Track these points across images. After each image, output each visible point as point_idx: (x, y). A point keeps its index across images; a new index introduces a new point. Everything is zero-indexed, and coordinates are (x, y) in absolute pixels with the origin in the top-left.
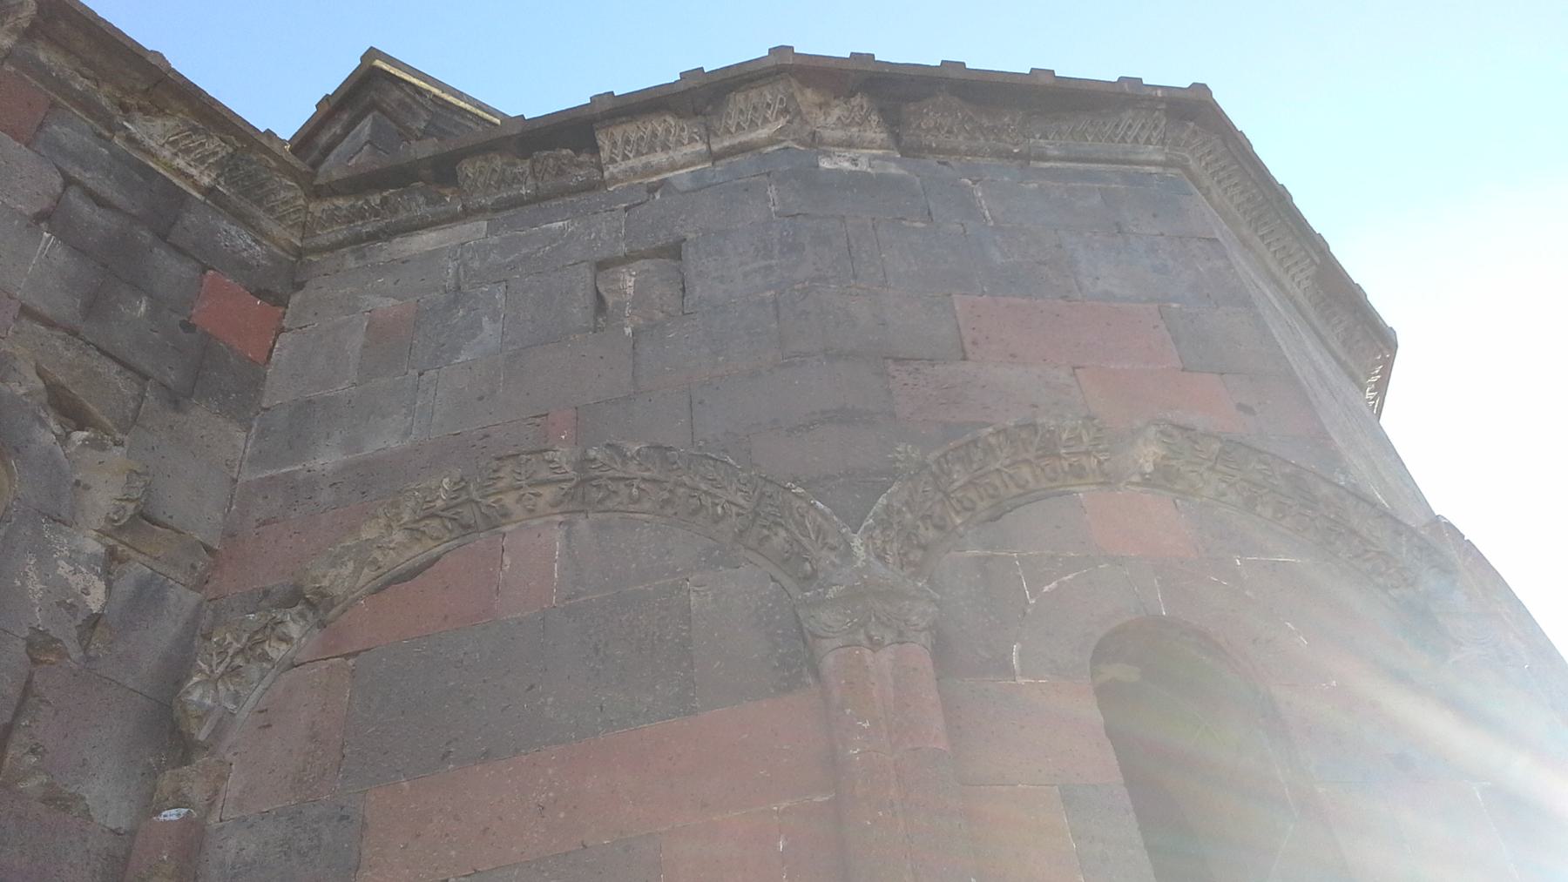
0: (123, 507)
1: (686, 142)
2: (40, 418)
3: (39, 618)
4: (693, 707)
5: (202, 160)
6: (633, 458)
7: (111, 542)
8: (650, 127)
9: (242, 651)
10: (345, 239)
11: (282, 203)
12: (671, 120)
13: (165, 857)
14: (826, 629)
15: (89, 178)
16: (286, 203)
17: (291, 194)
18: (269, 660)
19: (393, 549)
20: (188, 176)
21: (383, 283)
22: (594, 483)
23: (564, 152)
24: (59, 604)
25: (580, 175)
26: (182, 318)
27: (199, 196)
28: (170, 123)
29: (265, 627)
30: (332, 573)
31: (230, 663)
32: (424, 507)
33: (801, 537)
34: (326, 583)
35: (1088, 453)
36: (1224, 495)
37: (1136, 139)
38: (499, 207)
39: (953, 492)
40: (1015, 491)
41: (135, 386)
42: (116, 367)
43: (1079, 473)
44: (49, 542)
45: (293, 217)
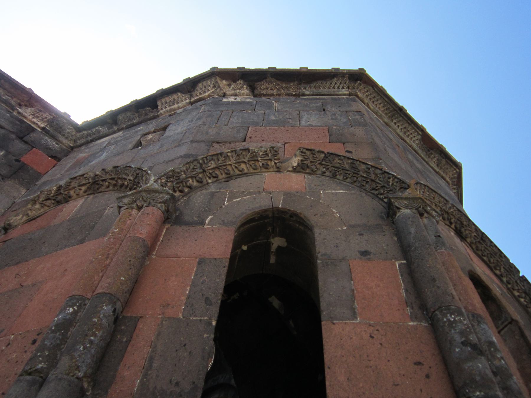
1: (184, 100)
5: (42, 120)
10: (84, 142)
12: (179, 94)
16: (68, 133)
17: (70, 131)
19: (34, 210)
20: (37, 124)
22: (96, 183)
23: (148, 108)
25: (152, 114)
27: (40, 130)
28: (33, 109)
30: (15, 218)
35: (271, 160)
36: (324, 173)
37: (338, 88)
40: (237, 172)
43: (266, 167)
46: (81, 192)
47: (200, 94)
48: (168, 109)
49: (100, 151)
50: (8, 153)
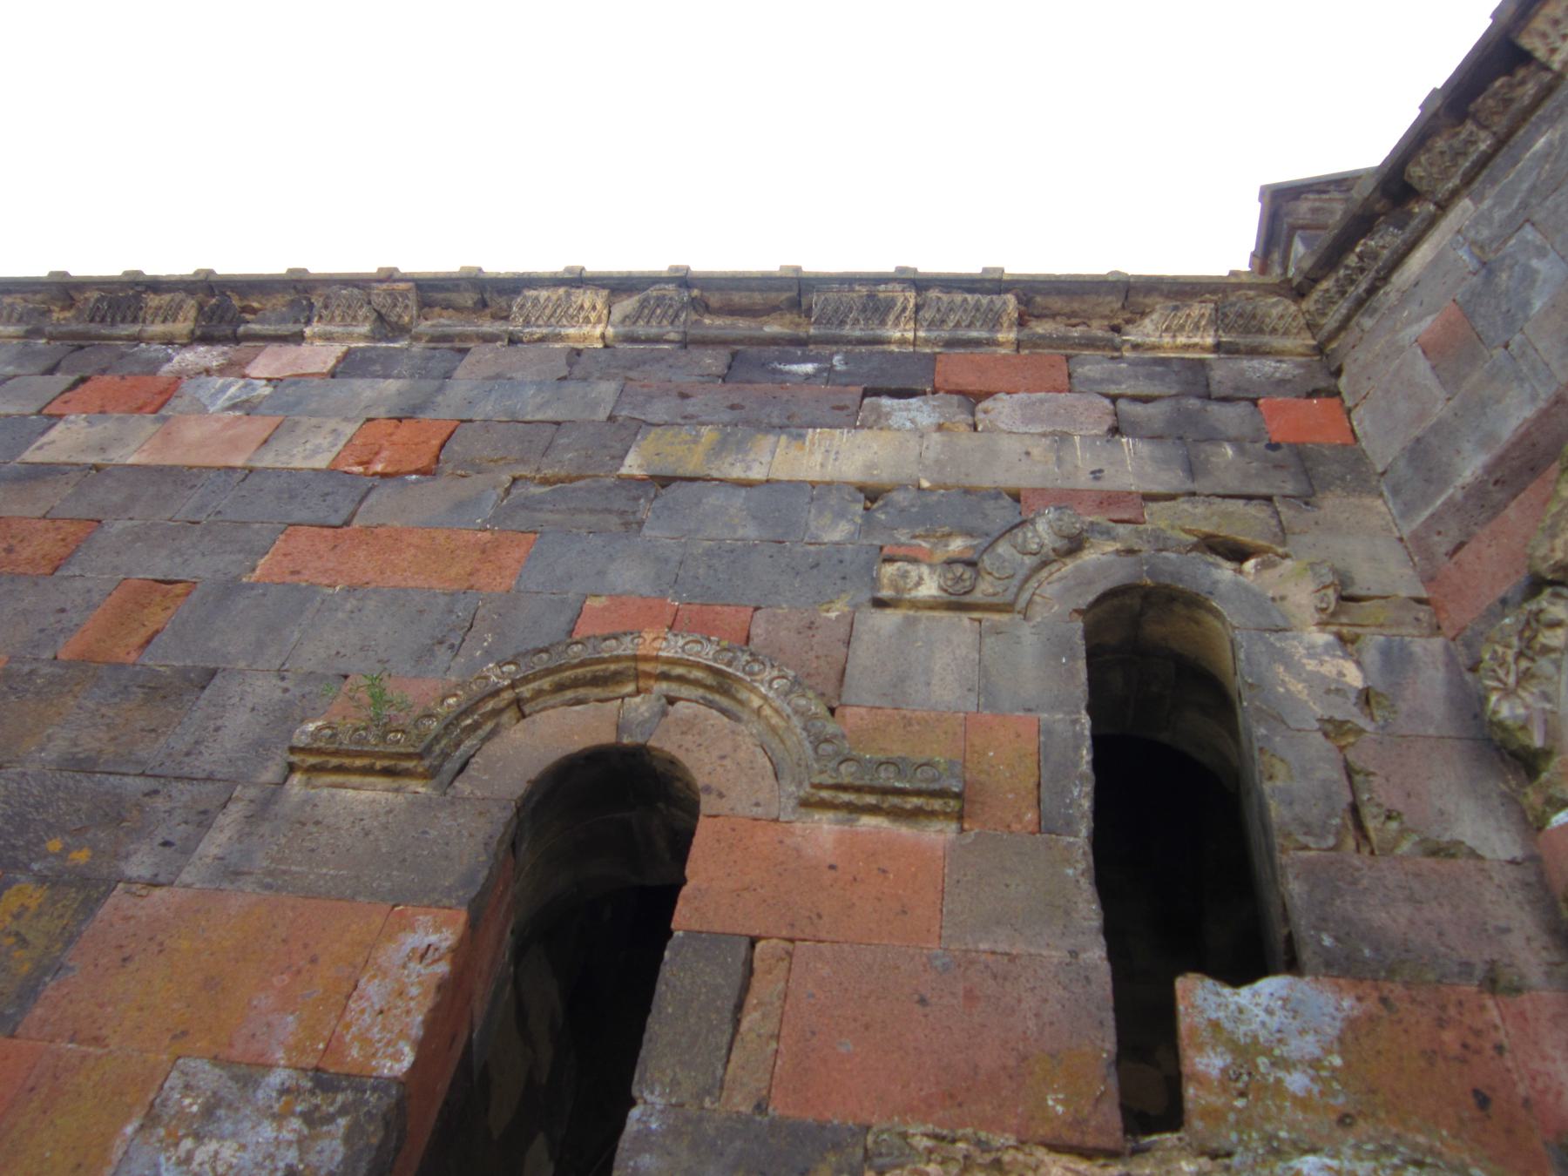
3: (1319, 711)
5: (1197, 327)
10: (1349, 309)
15: (1123, 388)
16: (1281, 317)
21: (1410, 314)
23: (1498, 83)
25: (1530, 89)
28: (1155, 316)
29: (1528, 623)
38: (1468, 180)
42: (1241, 503)
44: (1284, 649)
45: (1294, 324)
50: (1236, 442)
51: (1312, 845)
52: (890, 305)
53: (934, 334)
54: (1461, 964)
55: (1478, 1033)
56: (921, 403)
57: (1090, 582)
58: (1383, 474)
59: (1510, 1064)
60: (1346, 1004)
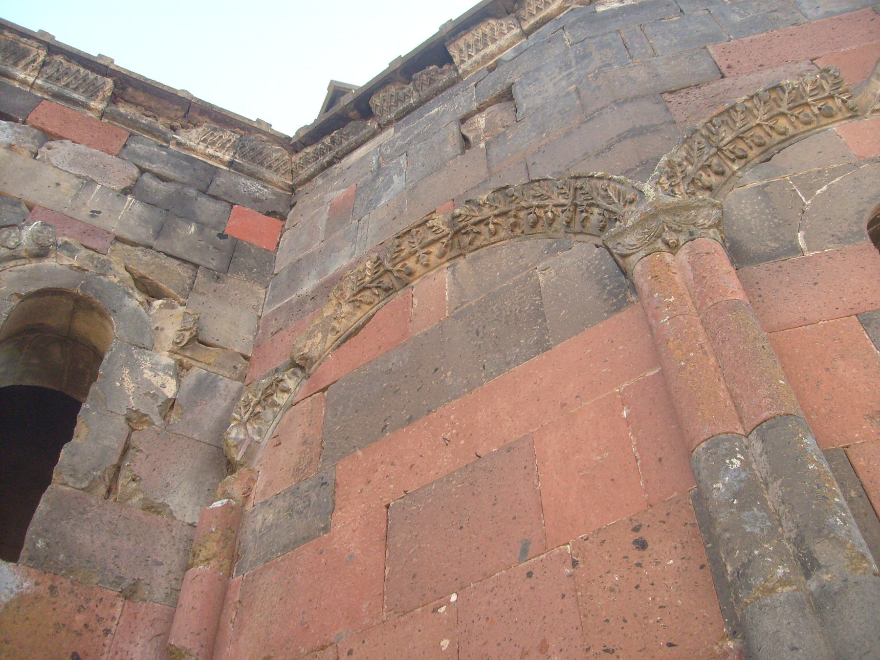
0: (182, 334)
1: (506, 32)
2: (128, 293)
3: (133, 403)
4: (548, 345)
5: (223, 146)
6: (485, 204)
7: (178, 357)
8: (480, 31)
9: (259, 402)
10: (315, 170)
11: (276, 161)
12: (492, 22)
13: (214, 529)
14: (630, 248)
15: (155, 168)
16: (278, 160)
17: (280, 154)
18: (278, 405)
22: (463, 231)
23: (431, 68)
24: (146, 394)
25: (445, 78)
26: (218, 232)
27: (225, 168)
28: (200, 130)
29: (272, 385)
30: (309, 343)
31: (253, 410)
32: (358, 284)
33: (608, 206)
34: (306, 350)
35: (831, 97)
38: (399, 118)
39: (725, 146)
40: (778, 138)
41: (190, 271)
42: (178, 262)
43: (828, 114)
44: (137, 360)
45: (284, 167)
46: (433, 258)
47: (538, 9)
48: (477, 57)
49: (378, 175)
50: (202, 226)
51: (70, 484)
52: (24, 54)
53: (47, 85)
54: (117, 577)
55: (100, 620)
56: (7, 126)
57: (38, 280)
58: (276, 275)
59: (107, 642)
60: (25, 585)
